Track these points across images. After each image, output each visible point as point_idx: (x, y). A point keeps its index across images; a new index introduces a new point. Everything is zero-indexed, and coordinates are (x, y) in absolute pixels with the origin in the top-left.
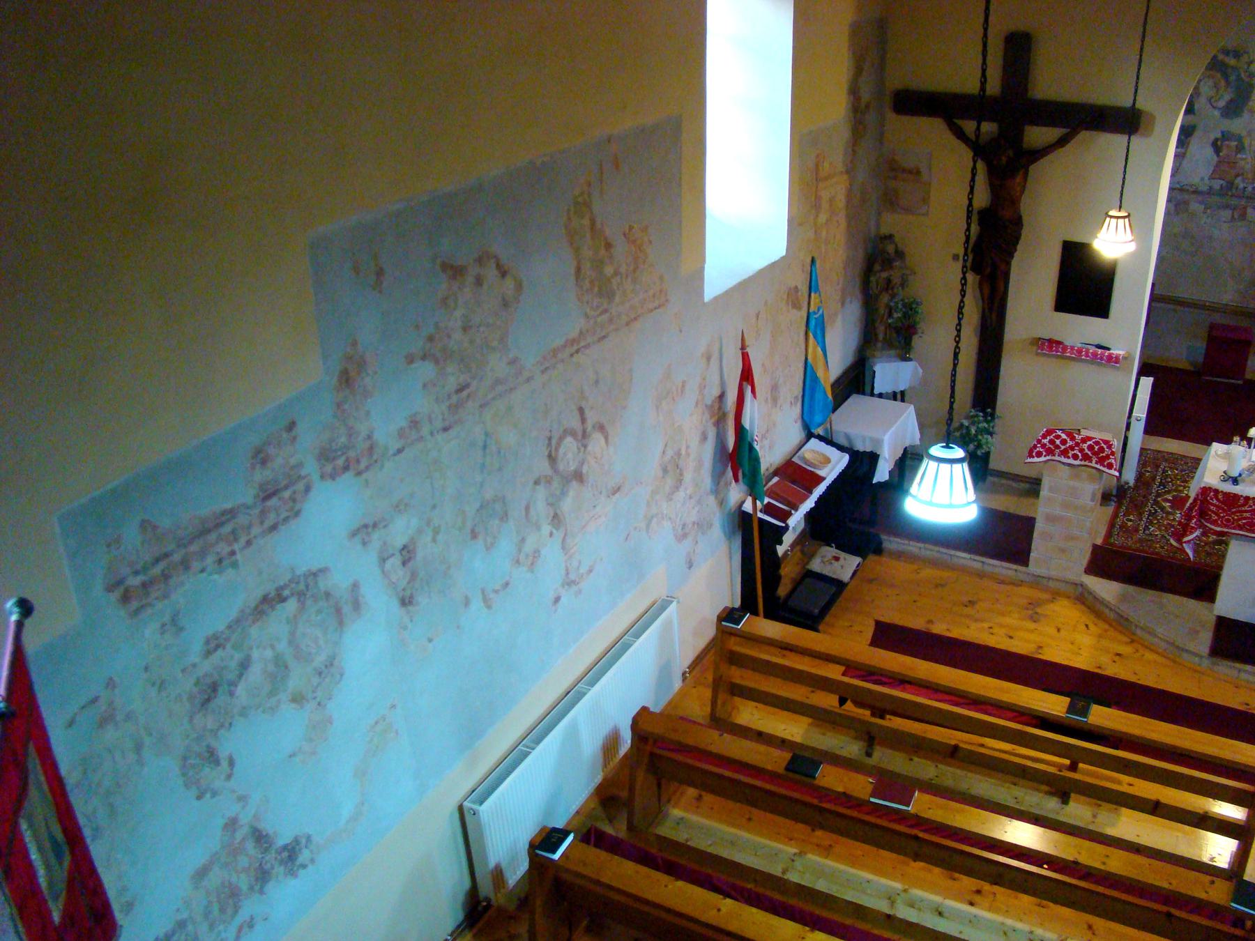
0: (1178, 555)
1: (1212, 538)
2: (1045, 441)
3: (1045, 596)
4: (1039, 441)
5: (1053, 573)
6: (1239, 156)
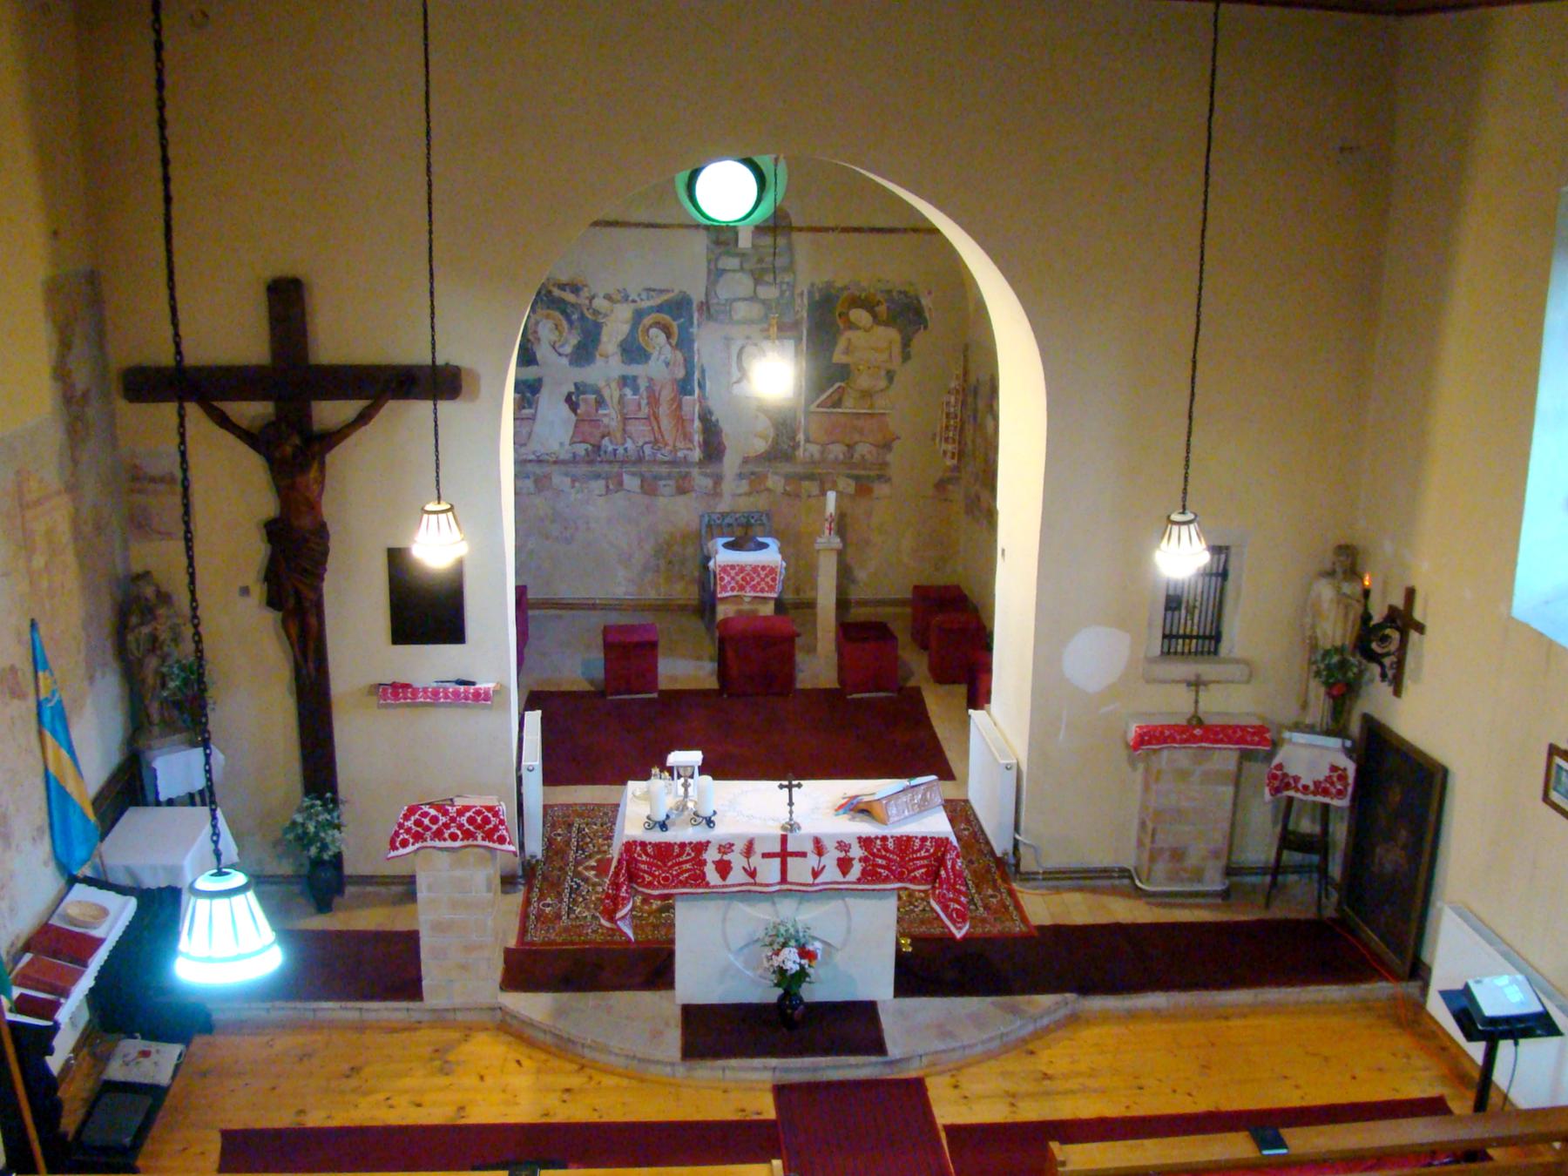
0: (617, 938)
1: (656, 904)
2: (409, 824)
3: (454, 1035)
4: (401, 826)
5: (458, 1001)
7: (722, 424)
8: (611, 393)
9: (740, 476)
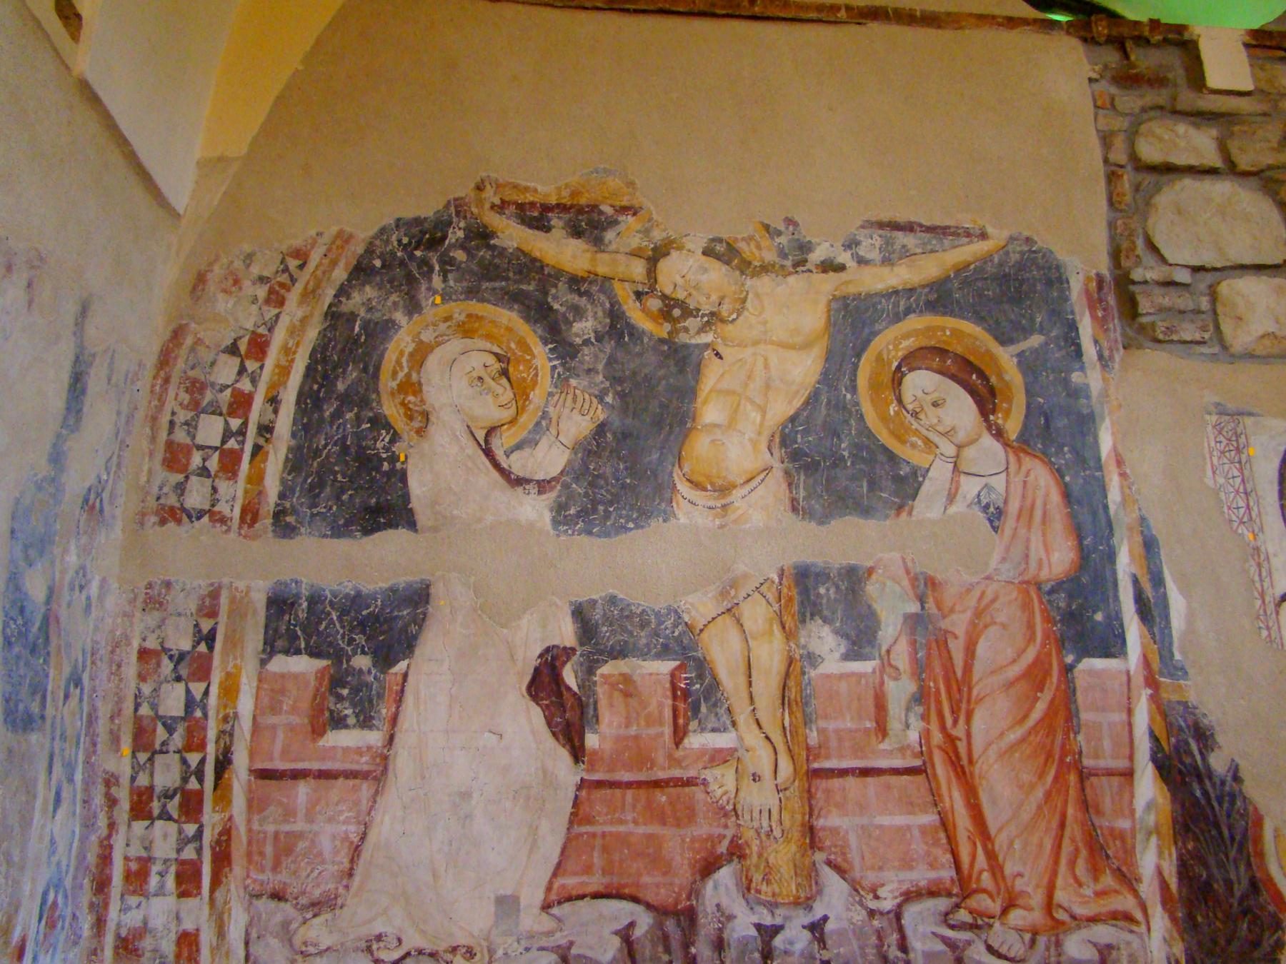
6: (696, 741)
7: (1251, 789)
8: (746, 651)
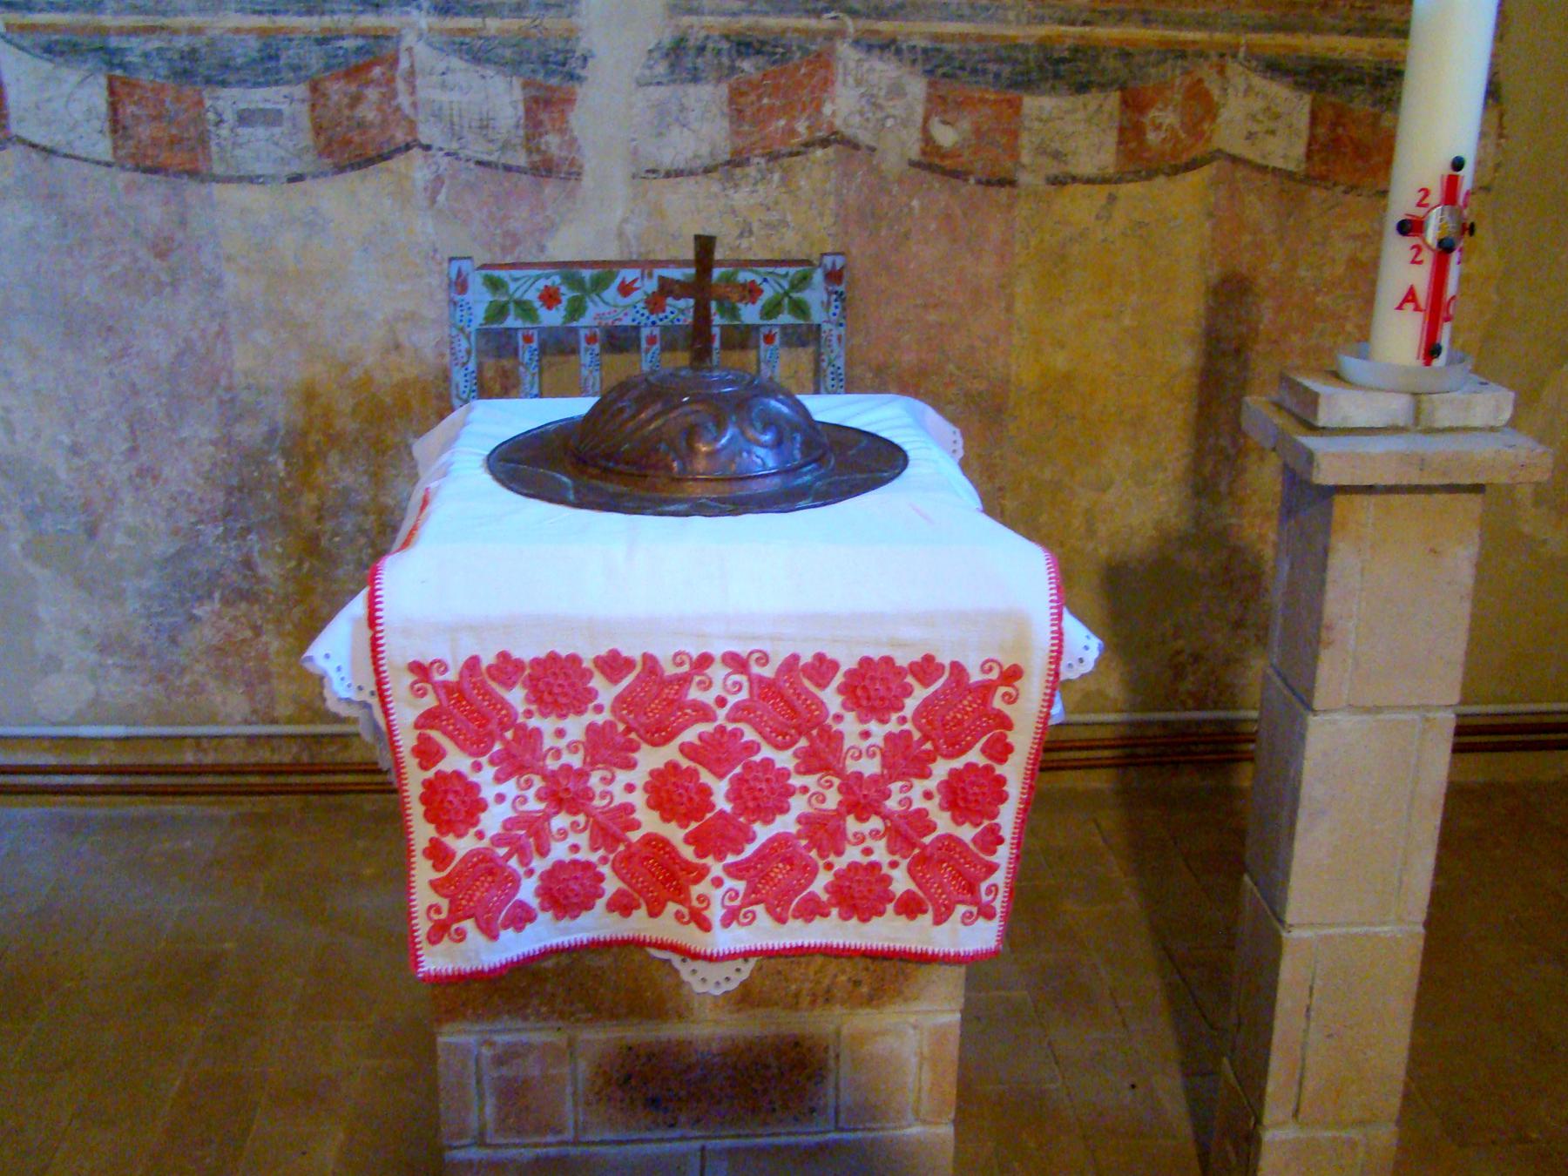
9: (679, 58)
